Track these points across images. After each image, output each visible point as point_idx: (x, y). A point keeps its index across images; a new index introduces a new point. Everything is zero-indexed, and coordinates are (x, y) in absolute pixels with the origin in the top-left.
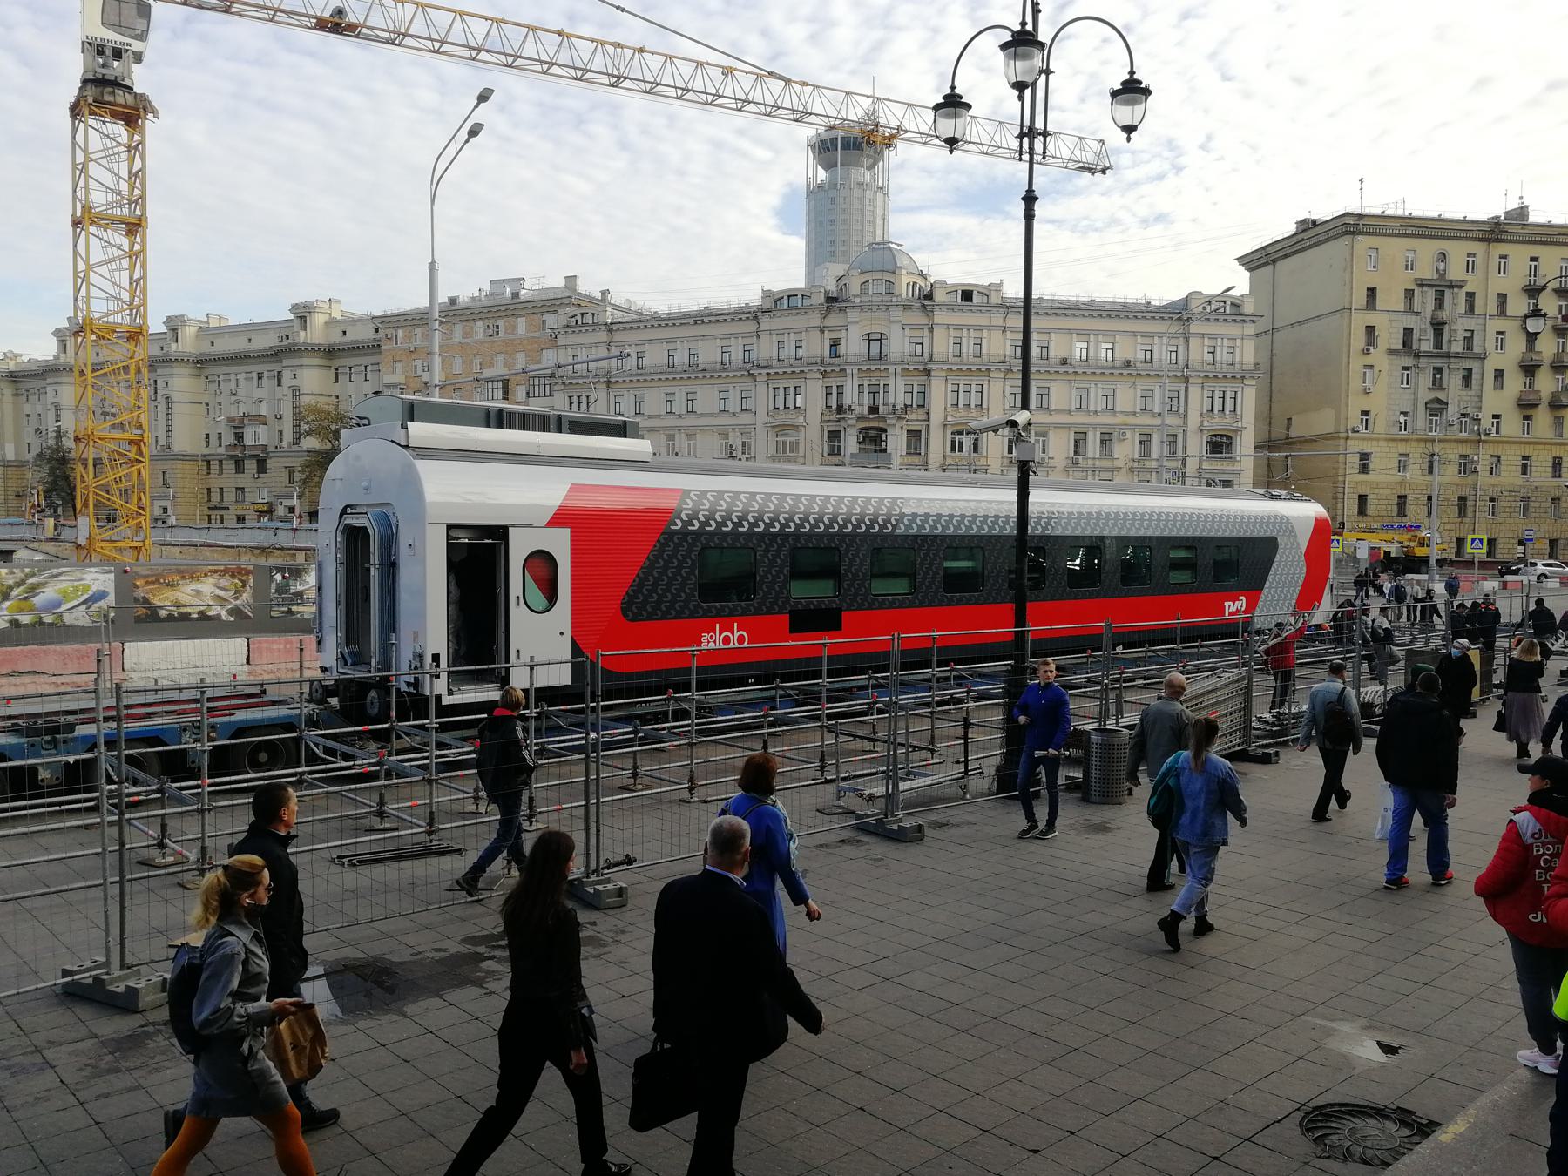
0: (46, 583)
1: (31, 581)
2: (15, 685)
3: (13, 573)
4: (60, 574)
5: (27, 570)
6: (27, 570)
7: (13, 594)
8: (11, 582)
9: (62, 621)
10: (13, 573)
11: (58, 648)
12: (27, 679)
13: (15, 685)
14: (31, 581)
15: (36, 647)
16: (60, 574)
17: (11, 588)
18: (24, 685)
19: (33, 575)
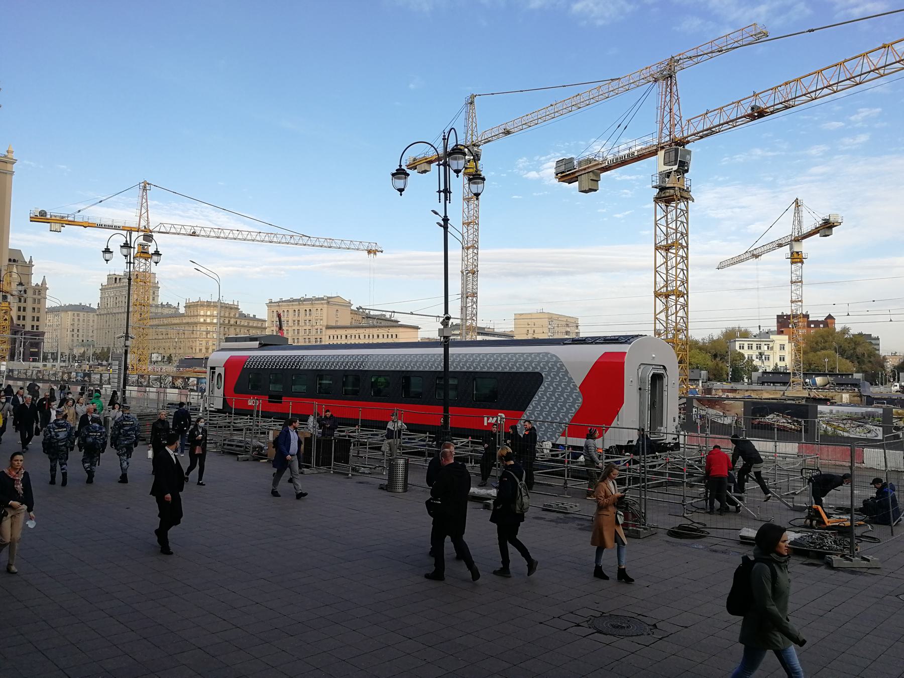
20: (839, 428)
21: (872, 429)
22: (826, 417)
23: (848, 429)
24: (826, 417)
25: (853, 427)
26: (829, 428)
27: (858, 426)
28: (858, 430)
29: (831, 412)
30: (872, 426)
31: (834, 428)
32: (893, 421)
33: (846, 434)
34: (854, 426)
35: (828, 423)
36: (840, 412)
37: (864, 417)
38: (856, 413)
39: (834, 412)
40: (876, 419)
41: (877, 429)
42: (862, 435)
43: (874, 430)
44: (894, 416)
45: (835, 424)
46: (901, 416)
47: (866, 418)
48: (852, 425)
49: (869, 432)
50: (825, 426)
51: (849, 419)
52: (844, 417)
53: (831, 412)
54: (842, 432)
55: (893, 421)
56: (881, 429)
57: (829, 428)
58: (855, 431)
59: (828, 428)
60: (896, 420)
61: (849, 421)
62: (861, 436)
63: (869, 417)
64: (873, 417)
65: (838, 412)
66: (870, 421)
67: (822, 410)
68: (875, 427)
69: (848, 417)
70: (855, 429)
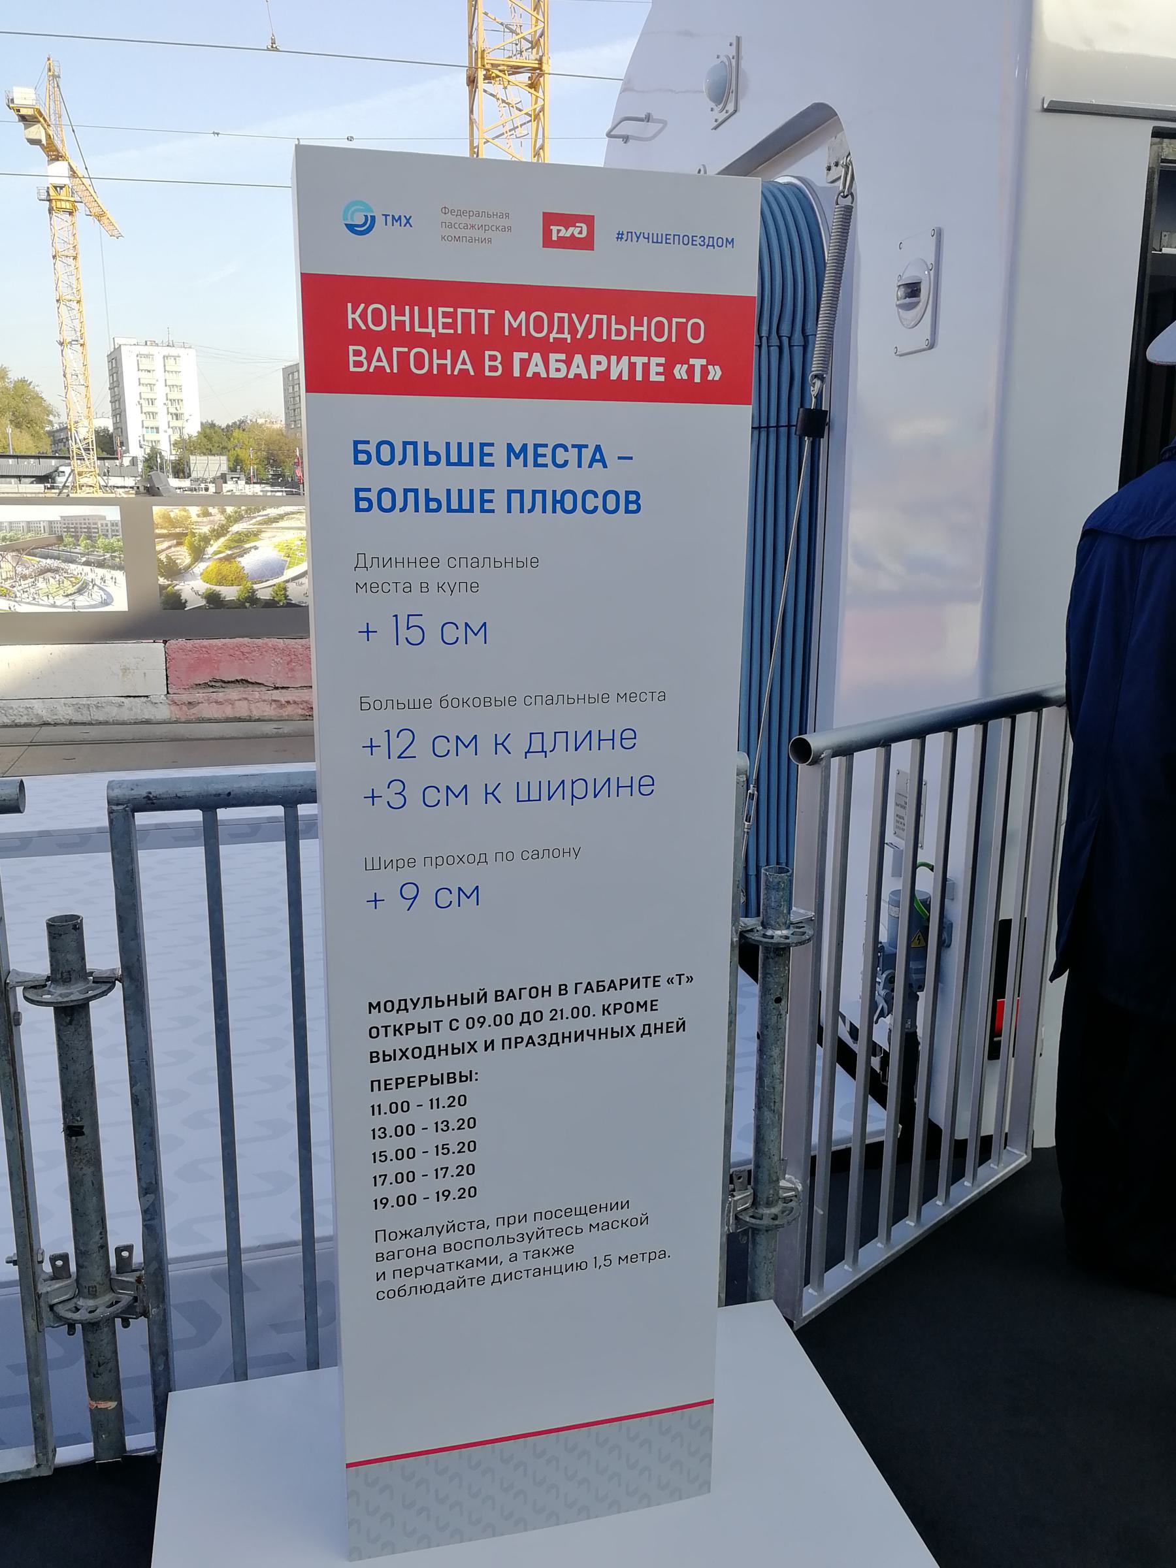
0: (260, 531)
1: (236, 528)
2: (220, 703)
3: (207, 514)
4: (281, 517)
5: (230, 510)
6: (230, 510)
7: (210, 550)
8: (205, 530)
9: (286, 597)
10: (207, 514)
11: (280, 643)
12: (234, 693)
13: (220, 703)
14: (236, 528)
15: (246, 640)
16: (281, 517)
17: (206, 540)
18: (231, 703)
19: (238, 518)
21: (91, 576)
23: (7, 585)
25: (24, 577)
27: (44, 571)
28: (41, 584)
30: (87, 569)
32: (159, 548)
34: (27, 572)
37: (60, 539)
38: (28, 523)
40: (101, 541)
41: (108, 577)
42: (58, 603)
43: (98, 582)
44: (157, 531)
46: (178, 530)
47: (67, 540)
48: (19, 569)
49: (80, 591)
55: (159, 548)
56: (120, 576)
58: (32, 590)
60: (166, 544)
62: (54, 606)
63: (77, 538)
64: (89, 538)
66: (79, 549)
68: (100, 572)
70: (34, 584)
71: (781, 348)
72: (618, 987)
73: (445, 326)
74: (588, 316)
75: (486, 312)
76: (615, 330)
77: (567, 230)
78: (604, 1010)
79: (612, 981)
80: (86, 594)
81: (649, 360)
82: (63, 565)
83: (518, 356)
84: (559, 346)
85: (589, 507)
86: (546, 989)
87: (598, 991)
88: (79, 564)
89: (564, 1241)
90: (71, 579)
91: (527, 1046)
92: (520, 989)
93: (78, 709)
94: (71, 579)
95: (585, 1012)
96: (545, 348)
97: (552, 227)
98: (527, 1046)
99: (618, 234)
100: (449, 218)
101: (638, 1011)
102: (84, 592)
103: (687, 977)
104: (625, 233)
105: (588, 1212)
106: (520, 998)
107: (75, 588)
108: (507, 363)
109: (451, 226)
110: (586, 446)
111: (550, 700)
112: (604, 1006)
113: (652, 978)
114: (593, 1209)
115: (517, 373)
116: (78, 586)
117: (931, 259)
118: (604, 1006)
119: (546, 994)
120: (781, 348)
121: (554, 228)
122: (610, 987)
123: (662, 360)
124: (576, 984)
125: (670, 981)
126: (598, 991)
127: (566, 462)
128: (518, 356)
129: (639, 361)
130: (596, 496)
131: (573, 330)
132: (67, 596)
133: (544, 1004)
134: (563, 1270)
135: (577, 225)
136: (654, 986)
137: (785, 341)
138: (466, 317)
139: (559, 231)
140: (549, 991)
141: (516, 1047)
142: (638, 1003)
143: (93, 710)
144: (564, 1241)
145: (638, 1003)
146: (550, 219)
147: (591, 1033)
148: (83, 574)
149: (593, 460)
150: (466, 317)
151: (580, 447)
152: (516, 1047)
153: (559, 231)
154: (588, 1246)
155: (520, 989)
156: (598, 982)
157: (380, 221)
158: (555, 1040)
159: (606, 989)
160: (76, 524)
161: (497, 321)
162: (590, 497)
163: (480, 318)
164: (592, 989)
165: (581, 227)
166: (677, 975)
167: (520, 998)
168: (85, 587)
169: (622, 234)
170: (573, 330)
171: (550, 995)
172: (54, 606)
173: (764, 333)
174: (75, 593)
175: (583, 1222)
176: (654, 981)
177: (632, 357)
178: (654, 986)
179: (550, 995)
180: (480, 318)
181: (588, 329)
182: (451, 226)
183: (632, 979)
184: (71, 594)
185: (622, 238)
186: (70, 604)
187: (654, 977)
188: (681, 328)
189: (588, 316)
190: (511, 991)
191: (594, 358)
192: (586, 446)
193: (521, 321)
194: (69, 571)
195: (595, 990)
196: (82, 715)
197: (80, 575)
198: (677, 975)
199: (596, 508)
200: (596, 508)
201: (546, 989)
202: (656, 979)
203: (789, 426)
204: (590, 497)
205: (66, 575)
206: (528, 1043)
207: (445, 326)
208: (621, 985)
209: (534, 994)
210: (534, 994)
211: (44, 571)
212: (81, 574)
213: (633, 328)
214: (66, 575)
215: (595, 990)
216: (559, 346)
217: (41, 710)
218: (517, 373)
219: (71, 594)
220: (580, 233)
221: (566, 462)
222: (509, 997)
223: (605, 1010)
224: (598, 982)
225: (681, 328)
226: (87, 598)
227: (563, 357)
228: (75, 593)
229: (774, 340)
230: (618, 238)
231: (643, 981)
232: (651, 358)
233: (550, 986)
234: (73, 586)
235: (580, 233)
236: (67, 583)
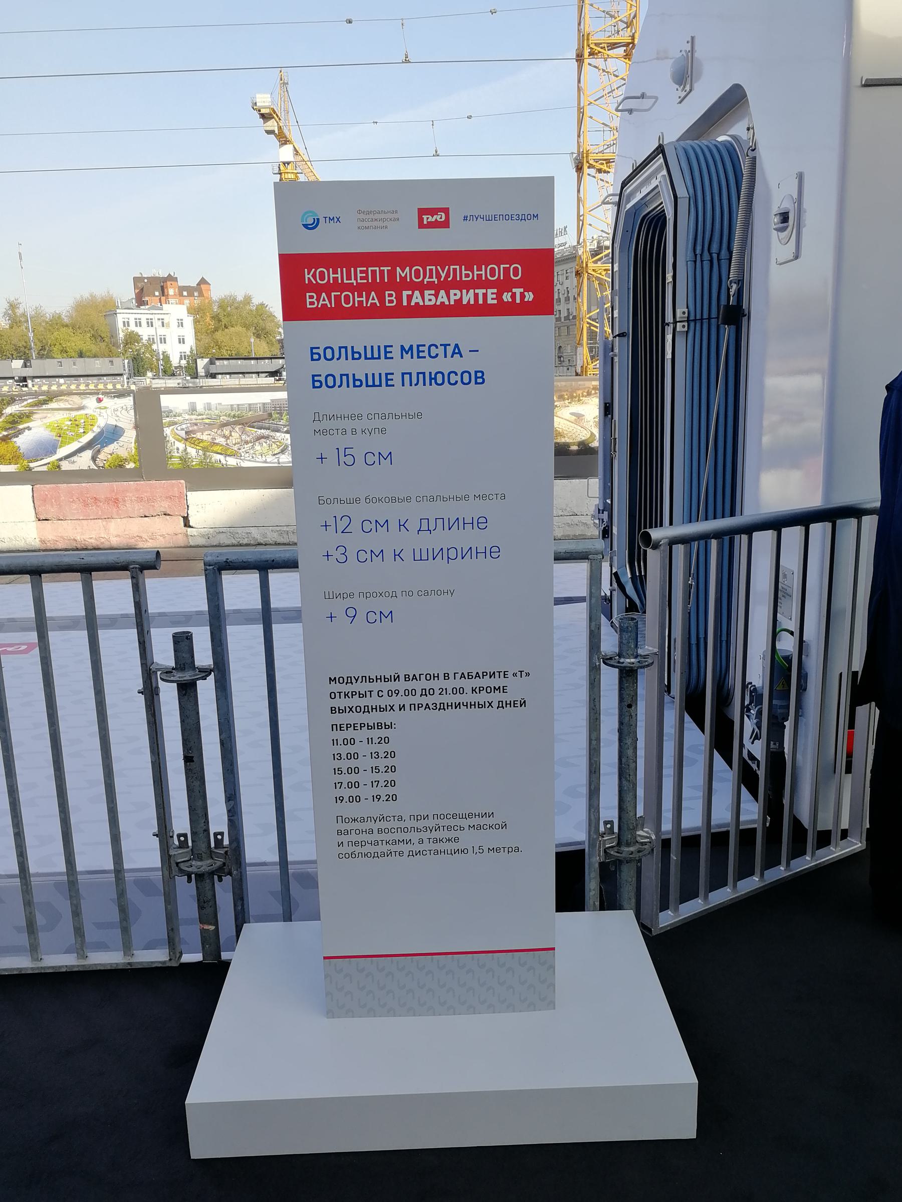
20: (216, 448)
22: (181, 423)
23: (235, 448)
24: (181, 423)
25: (247, 443)
26: (192, 451)
27: (259, 438)
28: (257, 447)
29: (193, 409)
31: (205, 449)
33: (232, 462)
34: (248, 439)
35: (189, 438)
36: (213, 407)
37: (270, 415)
38: (250, 404)
39: (200, 408)
45: (205, 437)
47: (275, 416)
48: (243, 437)
50: (181, 446)
51: (235, 423)
52: (224, 419)
53: (193, 409)
54: (222, 458)
57: (192, 451)
58: (252, 452)
59: (189, 450)
61: (237, 428)
62: (265, 462)
63: (281, 414)
65: (208, 407)
66: (282, 422)
67: (171, 407)
69: (234, 416)
70: (253, 447)
71: (711, 261)
72: (481, 677)
73: (362, 278)
74: (447, 267)
75: (386, 269)
76: (464, 274)
77: (432, 217)
78: (473, 690)
79: (477, 673)
80: (287, 453)
81: (487, 291)
82: (272, 434)
83: (405, 293)
84: (430, 286)
85: (452, 381)
86: (436, 675)
87: (468, 678)
88: (282, 432)
89: (452, 834)
90: (277, 443)
91: (425, 709)
92: (420, 675)
93: (281, 533)
94: (277, 443)
95: (461, 691)
96: (422, 288)
97: (423, 216)
98: (425, 709)
99: (465, 217)
100: (362, 216)
101: (494, 692)
102: (286, 452)
103: (526, 673)
104: (469, 216)
105: (467, 817)
106: (420, 680)
107: (279, 449)
108: (399, 298)
109: (363, 220)
110: (449, 345)
111: (432, 499)
112: (472, 688)
113: (503, 672)
114: (470, 815)
115: (405, 303)
116: (281, 448)
117: (795, 196)
118: (472, 688)
119: (436, 678)
120: (711, 261)
121: (425, 217)
122: (476, 676)
123: (495, 291)
124: (455, 673)
125: (515, 675)
126: (468, 678)
127: (437, 355)
128: (405, 293)
129: (480, 292)
130: (456, 374)
131: (438, 276)
132: (274, 455)
133: (435, 684)
134: (453, 853)
135: (439, 213)
136: (504, 677)
137: (715, 256)
138: (374, 272)
139: (428, 218)
140: (438, 677)
141: (418, 710)
142: (495, 687)
143: (291, 535)
144: (452, 834)
145: (495, 687)
146: (422, 212)
147: (465, 704)
148: (285, 439)
149: (454, 353)
150: (374, 272)
151: (445, 346)
152: (418, 710)
153: (428, 218)
154: (468, 839)
155: (420, 675)
156: (468, 673)
157: (322, 220)
158: (442, 707)
159: (474, 677)
160: (281, 404)
161: (392, 274)
162: (452, 375)
163: (382, 272)
164: (464, 677)
165: (441, 215)
166: (519, 671)
167: (420, 680)
168: (286, 449)
169: (467, 217)
170: (438, 276)
171: (438, 679)
172: (265, 462)
173: (698, 251)
174: (279, 453)
175: (465, 823)
176: (505, 675)
177: (476, 290)
178: (504, 677)
179: (438, 679)
180: (382, 272)
181: (448, 275)
182: (363, 220)
183: (490, 672)
184: (277, 454)
185: (467, 219)
186: (276, 460)
187: (504, 672)
188: (506, 271)
189: (447, 267)
190: (414, 675)
191: (452, 292)
192: (449, 345)
193: (399, 273)
194: (276, 438)
195: (467, 677)
196: (283, 538)
197: (282, 440)
198: (519, 671)
199: (456, 382)
200: (456, 382)
201: (436, 675)
202: (506, 673)
203: (709, 318)
204: (452, 375)
205: (273, 440)
206: (426, 708)
207: (362, 278)
208: (483, 675)
209: (428, 678)
210: (428, 678)
211: (259, 438)
212: (283, 439)
213: (476, 273)
214: (273, 440)
215: (467, 677)
216: (430, 286)
217: (257, 534)
218: (405, 303)
219: (277, 454)
220: (441, 218)
221: (437, 355)
222: (413, 679)
223: (473, 690)
224: (468, 673)
225: (506, 271)
226: (287, 456)
227: (433, 292)
228: (279, 453)
229: (706, 256)
230: (464, 219)
231: (497, 674)
232: (488, 290)
233: (438, 674)
234: (278, 448)
235: (441, 218)
236: (274, 446)
